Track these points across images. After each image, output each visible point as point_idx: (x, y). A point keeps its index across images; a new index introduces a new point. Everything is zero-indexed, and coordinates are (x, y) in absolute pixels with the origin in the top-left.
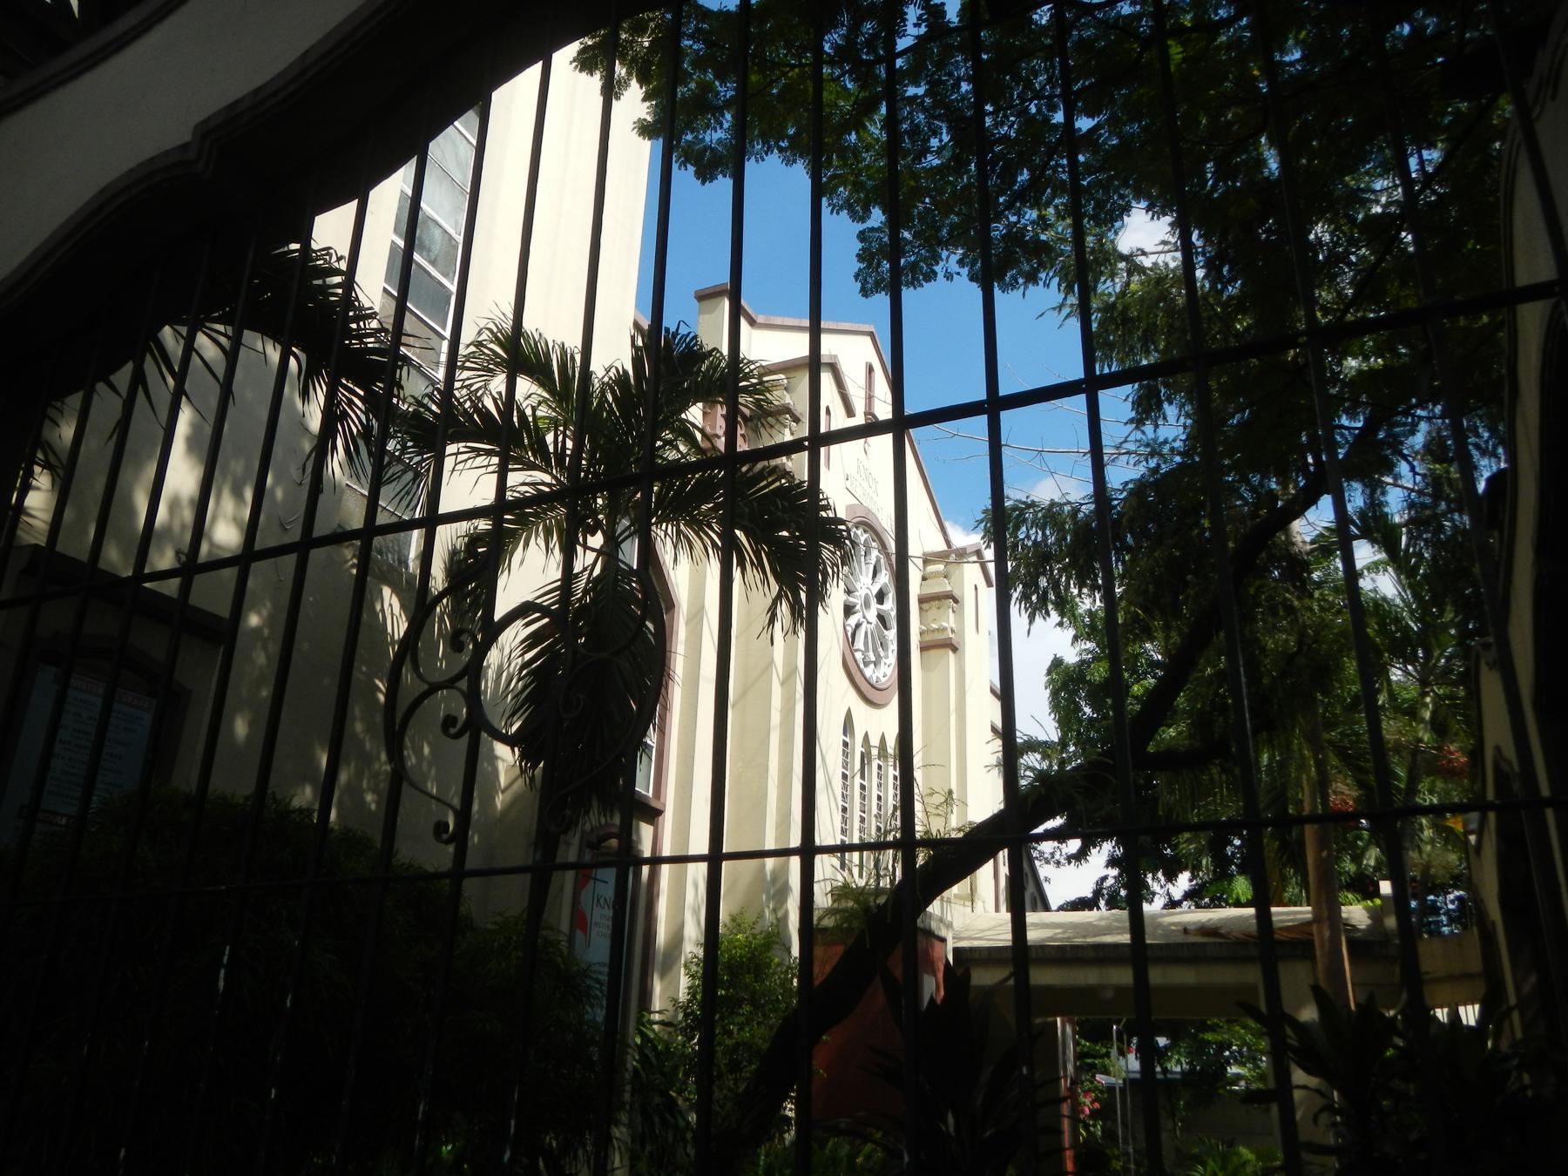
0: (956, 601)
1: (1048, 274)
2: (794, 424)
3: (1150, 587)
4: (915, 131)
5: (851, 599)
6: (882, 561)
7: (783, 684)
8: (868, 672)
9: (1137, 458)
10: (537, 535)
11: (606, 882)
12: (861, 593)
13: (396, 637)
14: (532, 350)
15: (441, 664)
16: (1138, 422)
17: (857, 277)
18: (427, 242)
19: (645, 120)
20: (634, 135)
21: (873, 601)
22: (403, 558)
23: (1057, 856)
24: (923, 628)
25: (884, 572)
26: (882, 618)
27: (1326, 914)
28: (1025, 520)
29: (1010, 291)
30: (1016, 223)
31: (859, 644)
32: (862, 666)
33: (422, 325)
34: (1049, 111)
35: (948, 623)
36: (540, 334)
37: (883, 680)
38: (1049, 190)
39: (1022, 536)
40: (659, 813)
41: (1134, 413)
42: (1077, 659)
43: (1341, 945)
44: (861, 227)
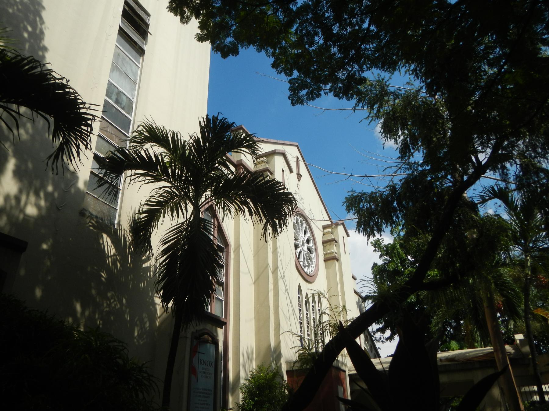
0: (336, 242)
1: (363, 104)
2: (271, 175)
3: (416, 218)
4: (308, 32)
5: (297, 242)
6: (307, 228)
7: (273, 273)
8: (306, 270)
9: (404, 170)
10: (168, 212)
11: (204, 354)
12: (301, 240)
13: (110, 254)
14: (160, 133)
15: (130, 265)
16: (402, 158)
17: (289, 98)
18: (120, 101)
19: (199, 34)
20: (195, 42)
21: (305, 243)
22: (112, 223)
23: (382, 339)
24: (325, 253)
25: (308, 232)
26: (309, 249)
27: (499, 348)
28: (362, 200)
29: (350, 100)
30: (351, 71)
31: (301, 259)
32: (303, 267)
33: (119, 132)
34: (361, 23)
35: (334, 250)
36: (163, 127)
37: (311, 273)
38: (363, 60)
39: (361, 207)
40: (225, 324)
41: (400, 154)
42: (383, 262)
43: (507, 360)
44: (290, 78)
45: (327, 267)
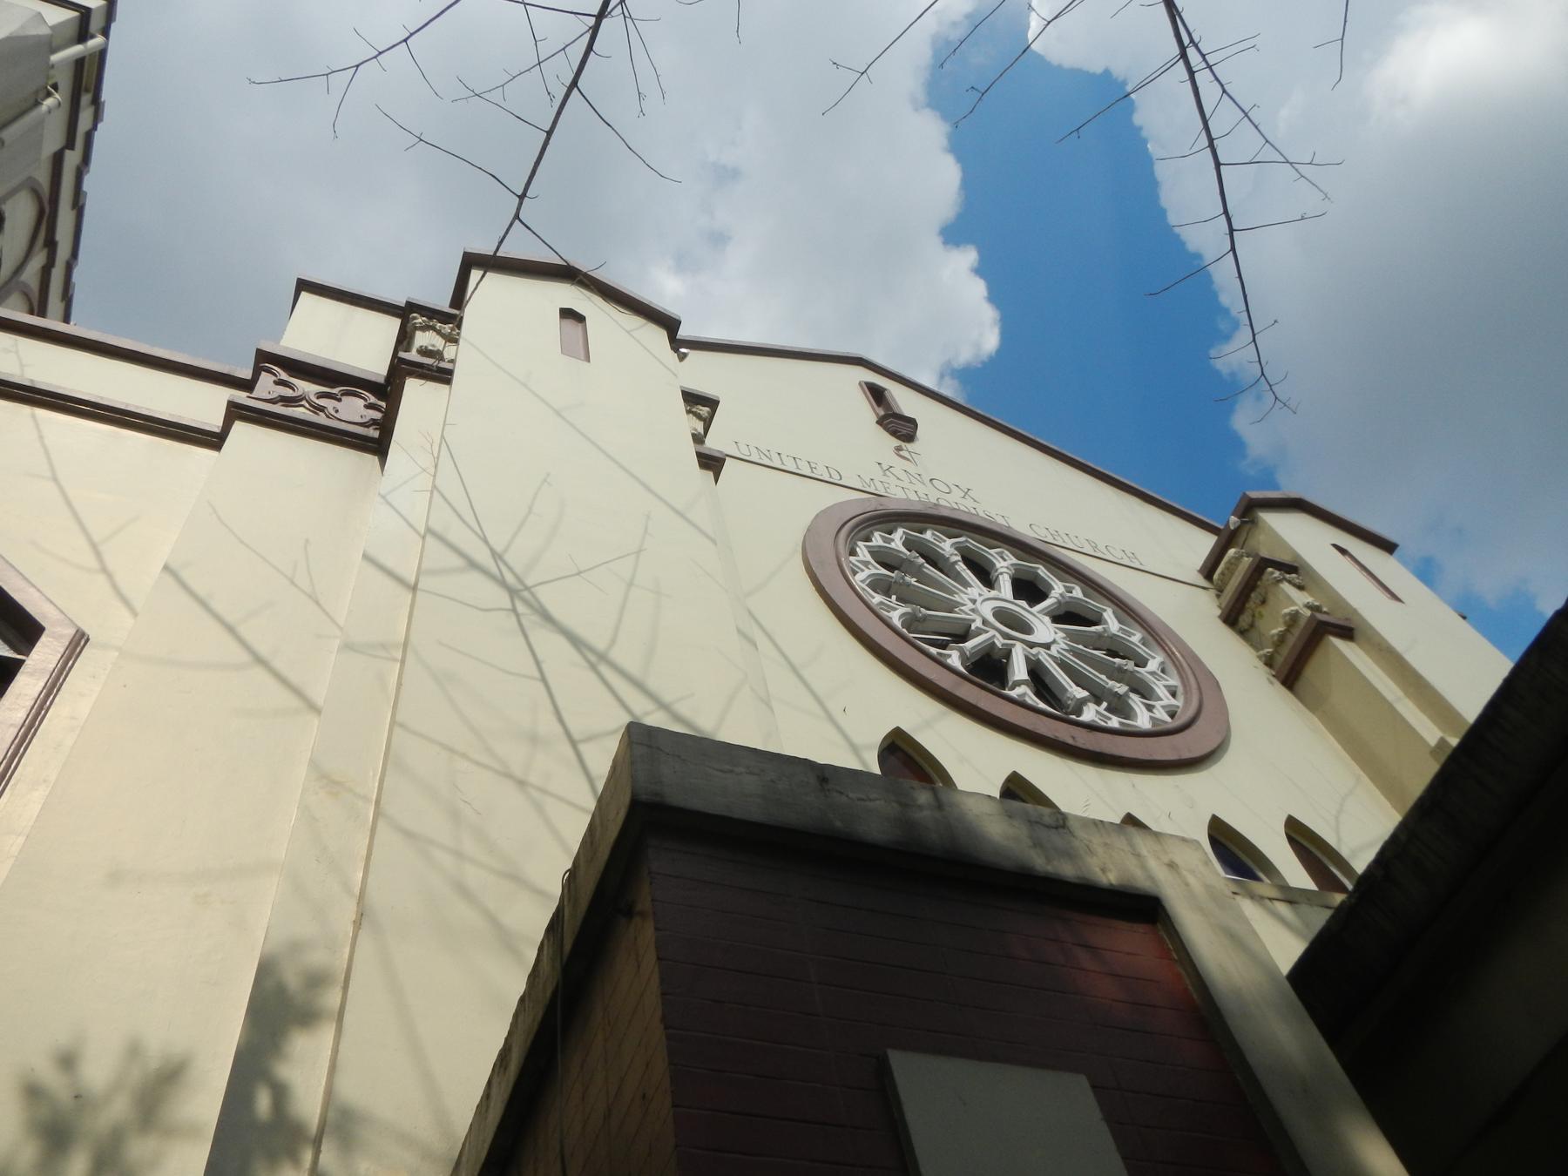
35: (1294, 603)
45: (1313, 703)
